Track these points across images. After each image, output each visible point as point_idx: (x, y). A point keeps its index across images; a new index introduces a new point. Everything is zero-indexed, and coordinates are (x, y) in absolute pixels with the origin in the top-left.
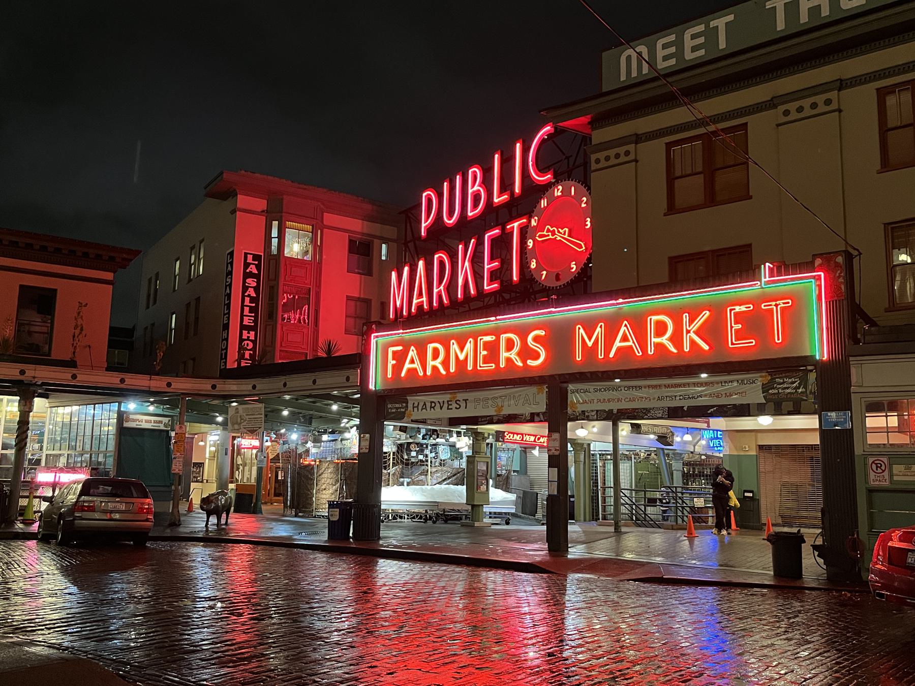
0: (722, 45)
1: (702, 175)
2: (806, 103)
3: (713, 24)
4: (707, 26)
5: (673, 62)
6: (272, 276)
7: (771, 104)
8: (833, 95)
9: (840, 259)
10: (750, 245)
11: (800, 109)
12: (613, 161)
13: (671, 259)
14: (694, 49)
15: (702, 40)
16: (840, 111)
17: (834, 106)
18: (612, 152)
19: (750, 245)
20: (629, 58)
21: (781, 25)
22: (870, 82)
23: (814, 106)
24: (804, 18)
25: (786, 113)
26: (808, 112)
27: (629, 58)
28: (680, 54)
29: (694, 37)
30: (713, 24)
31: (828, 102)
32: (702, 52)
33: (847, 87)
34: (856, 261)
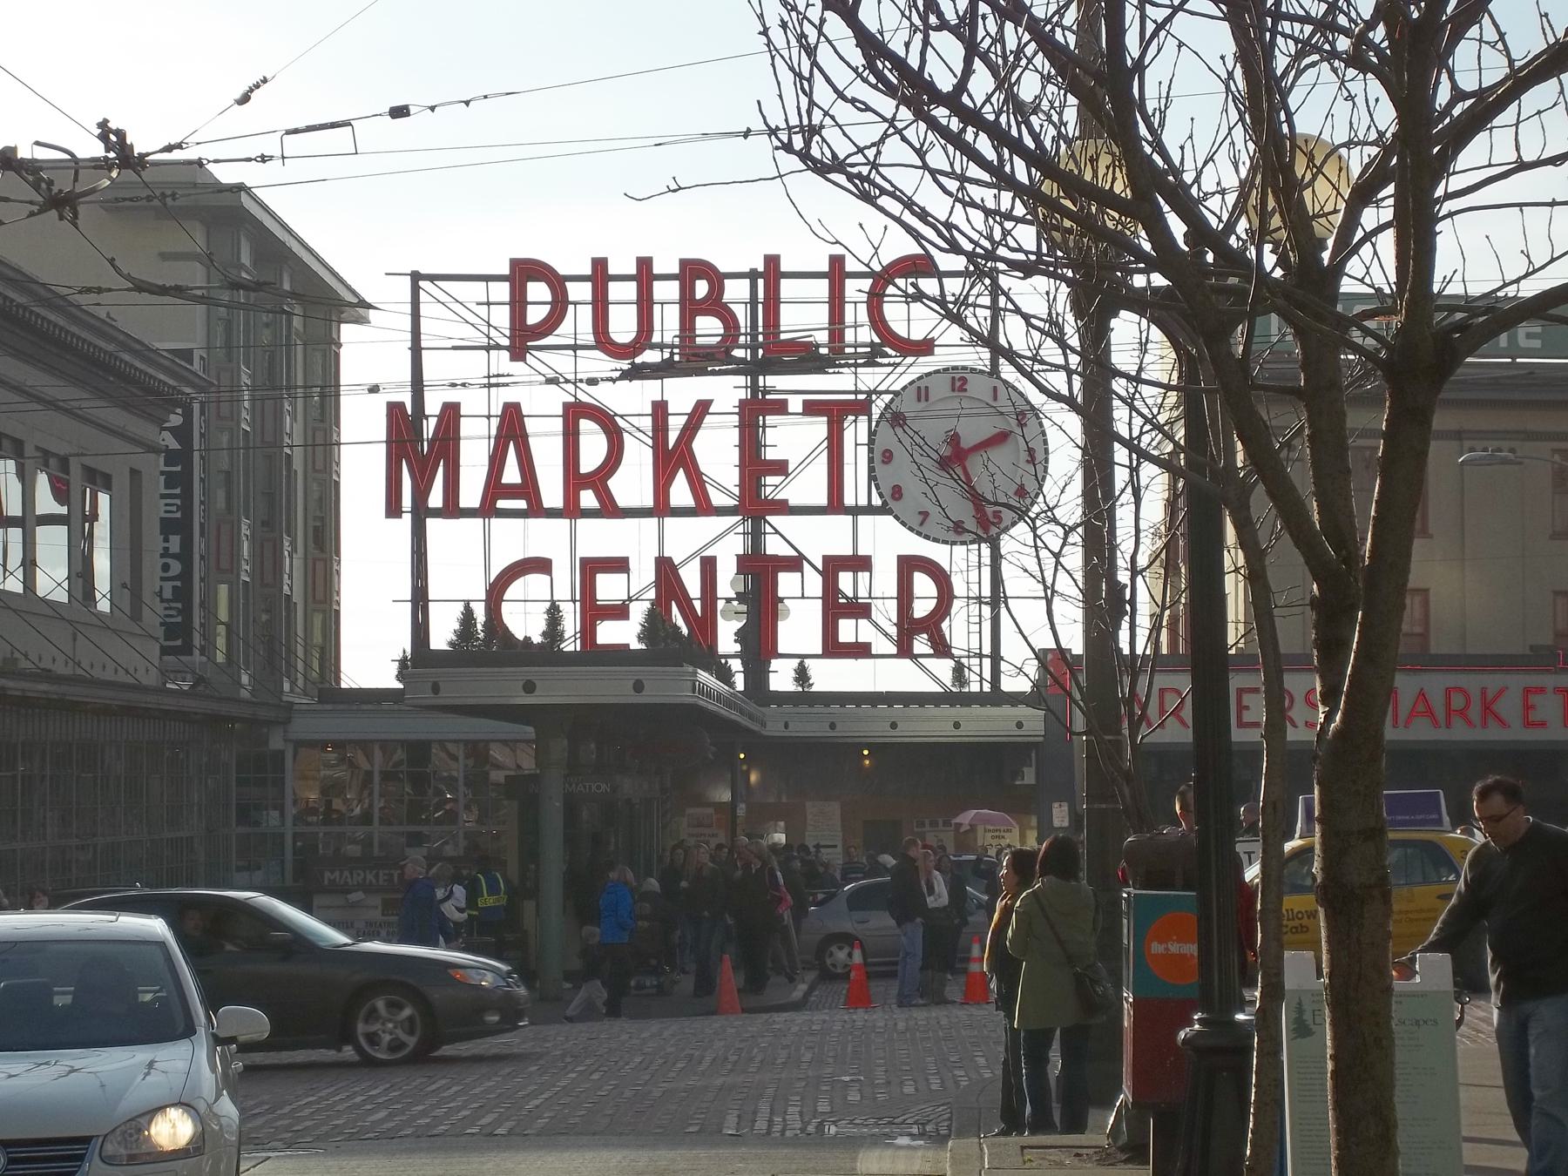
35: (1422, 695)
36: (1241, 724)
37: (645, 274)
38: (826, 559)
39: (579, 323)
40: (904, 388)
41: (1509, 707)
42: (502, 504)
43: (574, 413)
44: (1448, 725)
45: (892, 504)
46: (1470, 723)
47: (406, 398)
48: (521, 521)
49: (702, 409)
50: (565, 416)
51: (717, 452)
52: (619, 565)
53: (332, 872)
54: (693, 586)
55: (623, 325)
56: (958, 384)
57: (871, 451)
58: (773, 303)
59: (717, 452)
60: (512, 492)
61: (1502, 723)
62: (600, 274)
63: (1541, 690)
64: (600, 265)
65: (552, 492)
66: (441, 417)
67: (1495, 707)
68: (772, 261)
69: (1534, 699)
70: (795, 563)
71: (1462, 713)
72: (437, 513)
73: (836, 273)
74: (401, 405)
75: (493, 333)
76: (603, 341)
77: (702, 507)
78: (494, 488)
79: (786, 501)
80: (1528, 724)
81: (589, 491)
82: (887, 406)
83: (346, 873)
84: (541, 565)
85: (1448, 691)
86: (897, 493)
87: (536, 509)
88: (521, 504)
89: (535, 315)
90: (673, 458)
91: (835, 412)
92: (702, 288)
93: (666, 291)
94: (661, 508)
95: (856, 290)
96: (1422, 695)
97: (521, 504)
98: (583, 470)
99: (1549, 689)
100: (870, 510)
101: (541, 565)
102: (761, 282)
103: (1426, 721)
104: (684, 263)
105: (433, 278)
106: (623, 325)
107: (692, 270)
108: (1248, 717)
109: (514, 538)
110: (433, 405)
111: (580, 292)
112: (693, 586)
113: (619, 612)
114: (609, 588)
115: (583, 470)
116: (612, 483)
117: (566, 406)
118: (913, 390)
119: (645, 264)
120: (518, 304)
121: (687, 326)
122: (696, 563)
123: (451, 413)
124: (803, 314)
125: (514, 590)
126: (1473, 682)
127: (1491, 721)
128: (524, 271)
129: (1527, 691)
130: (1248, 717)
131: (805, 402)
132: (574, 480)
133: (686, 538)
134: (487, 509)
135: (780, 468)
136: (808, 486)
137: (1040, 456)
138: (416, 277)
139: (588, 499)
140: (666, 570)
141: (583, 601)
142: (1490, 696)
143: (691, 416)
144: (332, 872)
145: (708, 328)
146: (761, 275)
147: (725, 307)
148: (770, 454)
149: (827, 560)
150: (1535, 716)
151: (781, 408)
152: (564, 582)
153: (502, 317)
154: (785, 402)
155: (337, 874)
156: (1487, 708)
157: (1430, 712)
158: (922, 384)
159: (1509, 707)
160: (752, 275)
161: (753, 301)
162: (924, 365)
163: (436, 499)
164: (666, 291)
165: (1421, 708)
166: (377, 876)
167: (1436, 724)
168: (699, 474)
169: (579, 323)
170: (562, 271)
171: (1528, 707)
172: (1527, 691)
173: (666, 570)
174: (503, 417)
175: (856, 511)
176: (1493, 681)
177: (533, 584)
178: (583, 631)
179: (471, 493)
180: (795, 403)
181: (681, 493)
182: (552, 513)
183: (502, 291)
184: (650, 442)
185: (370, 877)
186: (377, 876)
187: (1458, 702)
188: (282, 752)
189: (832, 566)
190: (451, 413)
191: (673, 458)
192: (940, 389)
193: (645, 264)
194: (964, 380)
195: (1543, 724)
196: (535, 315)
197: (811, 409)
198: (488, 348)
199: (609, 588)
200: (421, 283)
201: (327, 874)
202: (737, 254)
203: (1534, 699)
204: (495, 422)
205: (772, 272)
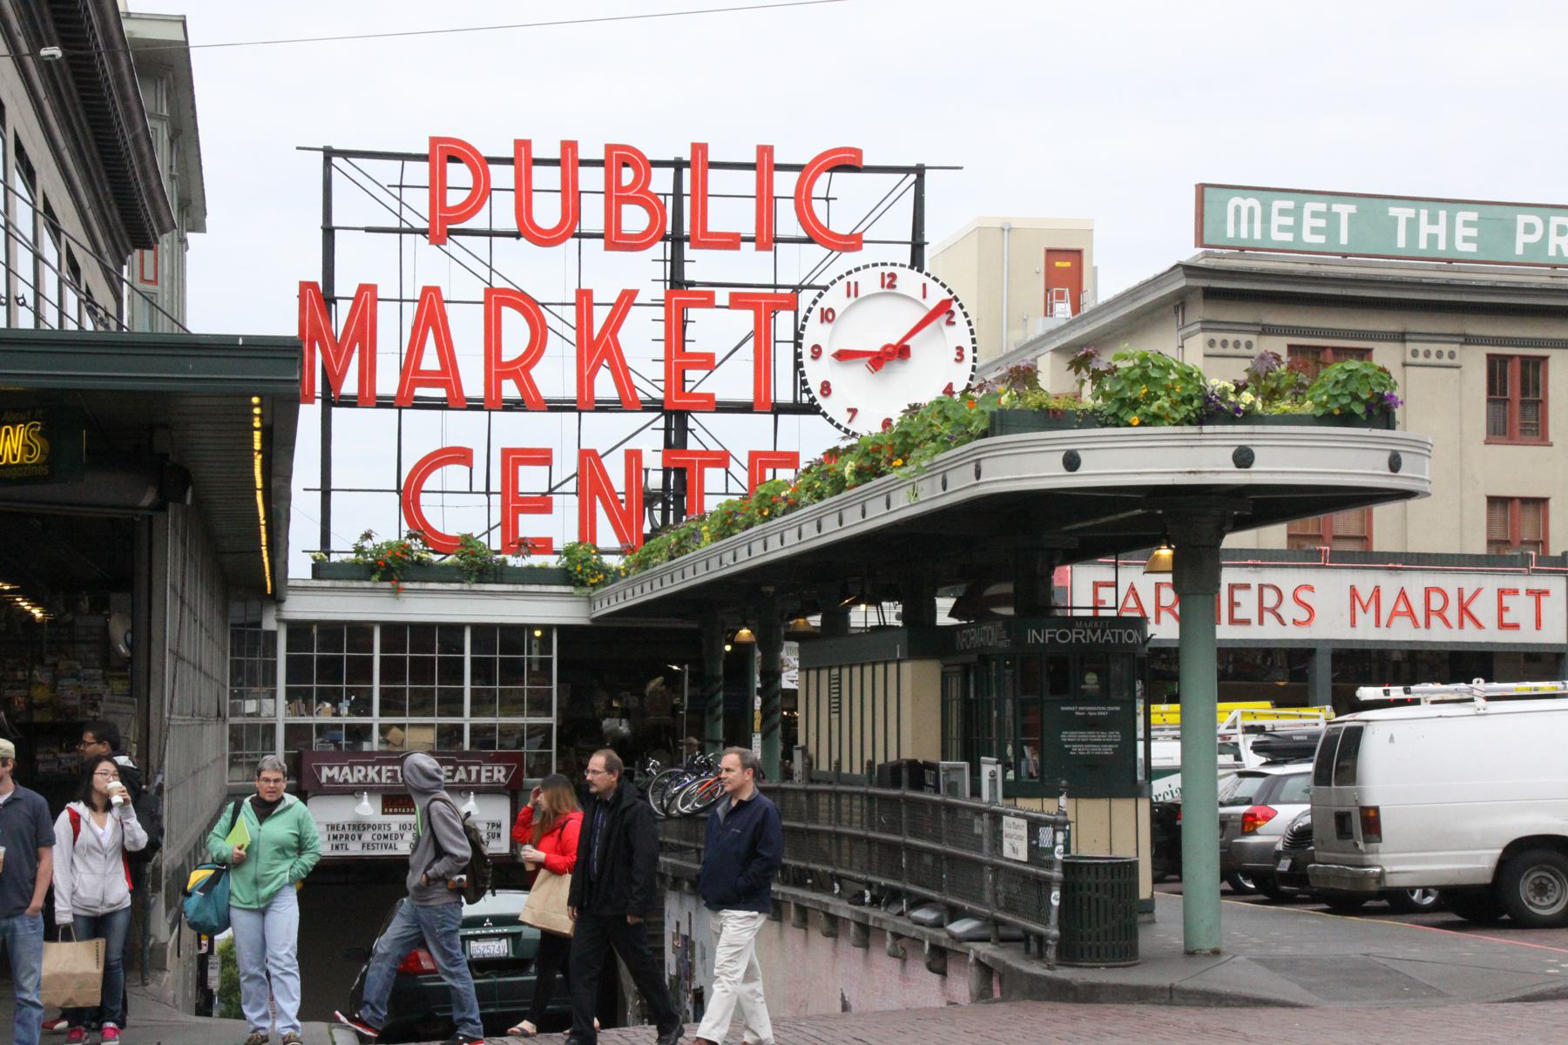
0: (1344, 239)
2: (1434, 348)
3: (1336, 208)
4: (1329, 208)
6: (149, 275)
7: (1401, 337)
11: (1427, 354)
12: (1230, 350)
14: (1315, 231)
15: (1321, 223)
18: (1231, 337)
20: (1238, 210)
21: (1401, 242)
23: (1439, 354)
24: (1423, 244)
25: (1415, 353)
26: (1433, 359)
27: (1238, 210)
28: (1297, 228)
29: (1315, 215)
32: (1321, 239)
35: (1403, 594)
36: (1233, 621)
37: (569, 159)
38: (753, 455)
39: (501, 211)
40: (833, 282)
41: (1484, 608)
42: (420, 392)
43: (497, 300)
44: (1428, 625)
45: (820, 400)
47: (317, 277)
48: (439, 412)
49: (627, 299)
50: (487, 303)
51: (642, 342)
52: (543, 457)
53: (331, 768)
54: (619, 484)
55: (547, 212)
56: (887, 280)
57: (797, 345)
58: (701, 195)
59: (642, 342)
60: (431, 380)
61: (1479, 626)
62: (523, 158)
63: (1516, 592)
64: (523, 145)
65: (473, 386)
66: (356, 300)
67: (1472, 608)
68: (699, 149)
69: (1507, 600)
70: (721, 459)
71: (1440, 613)
72: (349, 402)
73: (764, 164)
74: (314, 285)
75: (406, 214)
76: (526, 230)
77: (626, 403)
78: (411, 372)
79: (711, 396)
80: (1502, 625)
81: (513, 385)
82: (815, 302)
83: (346, 769)
84: (462, 456)
85: (1428, 591)
86: (826, 389)
87: (456, 402)
88: (441, 393)
89: (454, 199)
90: (597, 349)
91: (763, 303)
92: (628, 176)
93: (591, 179)
94: (585, 403)
95: (785, 183)
96: (1403, 594)
97: (441, 393)
98: (504, 359)
99: (1522, 592)
100: (796, 408)
101: (462, 456)
102: (687, 172)
103: (1407, 620)
104: (609, 148)
105: (346, 154)
106: (547, 212)
107: (619, 157)
108: (1239, 614)
109: (427, 431)
110: (345, 286)
111: (502, 176)
112: (619, 484)
113: (542, 504)
114: (531, 480)
115: (504, 359)
116: (533, 372)
117: (490, 291)
118: (842, 284)
119: (569, 146)
120: (438, 186)
121: (612, 217)
122: (620, 452)
123: (367, 296)
124: (730, 207)
125: (432, 482)
126: (1450, 582)
127: (1466, 620)
128: (447, 152)
129: (1501, 592)
130: (1239, 614)
131: (732, 295)
132: (496, 368)
133: (605, 432)
134: (403, 401)
135: (707, 362)
136: (733, 381)
137: (968, 354)
138: (329, 154)
139: (510, 390)
140: (589, 461)
141: (504, 493)
142: (1466, 599)
143: (616, 306)
144: (331, 768)
145: (635, 219)
146: (687, 164)
147: (655, 196)
148: (689, 348)
149: (753, 455)
150: (1508, 618)
151: (708, 302)
152: (487, 468)
153: (420, 201)
154: (711, 295)
155: (336, 770)
156: (1464, 609)
157: (1410, 613)
158: (852, 279)
159: (1484, 608)
160: (678, 165)
161: (678, 195)
162: (848, 260)
163: (350, 386)
164: (591, 179)
165: (1402, 608)
166: (379, 773)
167: (1416, 623)
168: (626, 369)
169: (501, 211)
170: (486, 152)
171: (1502, 609)
172: (1501, 592)
173: (589, 461)
174: (421, 302)
175: (778, 409)
176: (1469, 582)
177: (453, 475)
178: (504, 524)
179: (387, 382)
180: (722, 296)
181: (605, 386)
182: (474, 406)
183: (419, 172)
184: (572, 335)
185: (372, 772)
186: (379, 773)
187: (1436, 602)
188: (274, 634)
189: (759, 462)
190: (367, 296)
191: (597, 349)
192: (870, 282)
193: (569, 146)
194: (893, 276)
195: (1516, 626)
196: (454, 199)
197: (737, 302)
198: (400, 231)
199: (531, 480)
200: (336, 160)
201: (326, 772)
202: (663, 141)
203: (1507, 600)
204: (410, 310)
205: (697, 162)
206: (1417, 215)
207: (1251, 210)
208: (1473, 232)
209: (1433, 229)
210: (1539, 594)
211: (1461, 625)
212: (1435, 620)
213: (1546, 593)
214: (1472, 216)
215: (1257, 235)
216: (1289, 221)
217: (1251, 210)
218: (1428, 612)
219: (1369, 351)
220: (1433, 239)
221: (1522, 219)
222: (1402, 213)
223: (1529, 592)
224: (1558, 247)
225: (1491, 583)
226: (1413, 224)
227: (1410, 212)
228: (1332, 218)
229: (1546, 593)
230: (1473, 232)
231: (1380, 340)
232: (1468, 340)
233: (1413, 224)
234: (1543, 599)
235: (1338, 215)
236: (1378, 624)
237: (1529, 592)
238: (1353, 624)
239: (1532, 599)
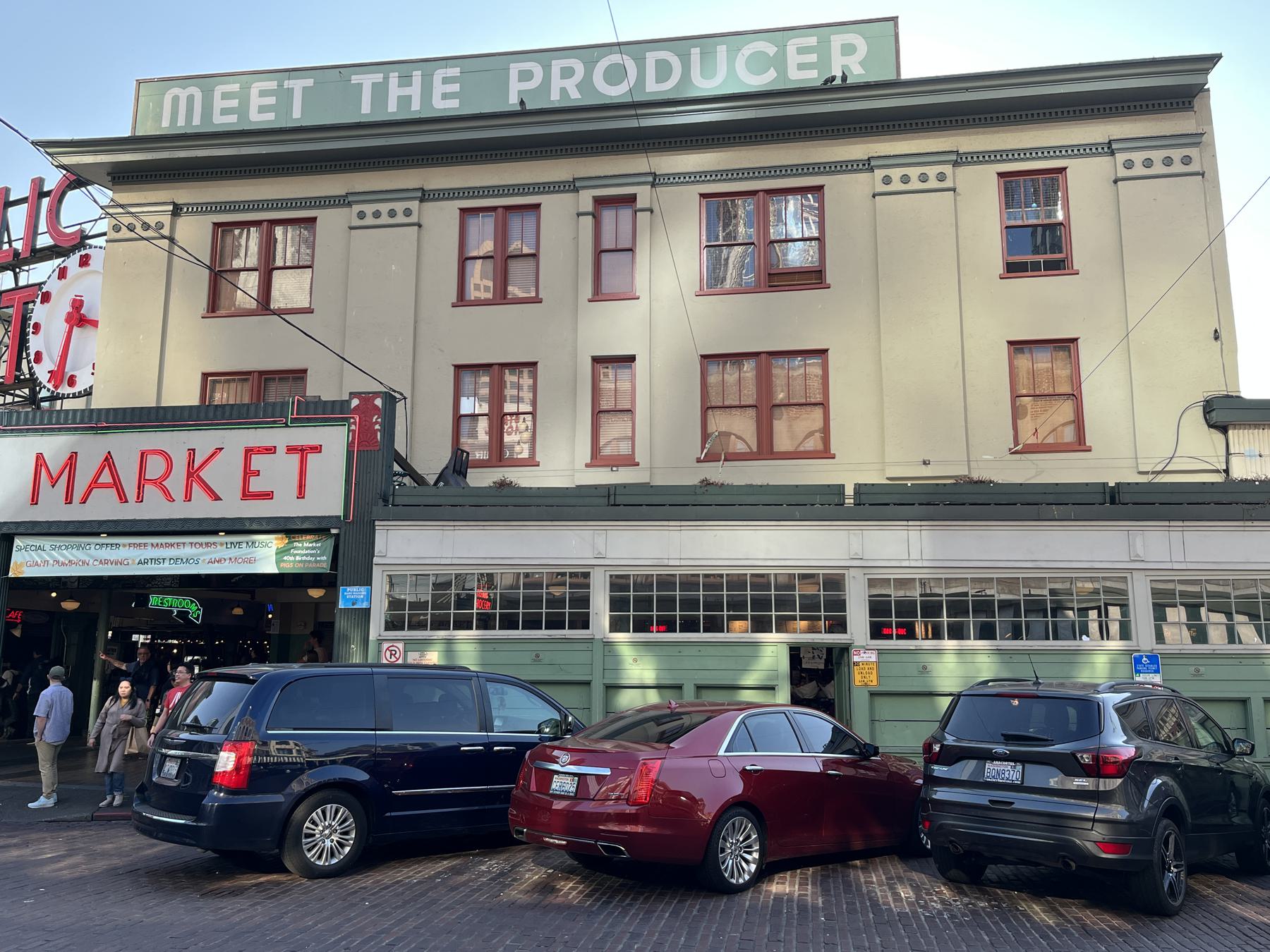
0: (297, 114)
1: (257, 273)
2: (384, 208)
3: (286, 84)
4: (280, 85)
5: (233, 119)
7: (343, 201)
8: (414, 205)
9: (378, 402)
10: (305, 371)
13: (205, 376)
14: (262, 109)
15: (271, 100)
16: (420, 226)
17: (413, 219)
19: (305, 371)
20: (176, 99)
22: (453, 199)
23: (392, 213)
24: (392, 107)
26: (385, 219)
27: (176, 99)
28: (243, 110)
30: (286, 84)
31: (408, 213)
32: (271, 116)
33: (429, 200)
34: (400, 406)
35: (108, 461)
44: (140, 499)
46: (166, 492)
63: (271, 450)
69: (257, 462)
71: (159, 483)
80: (247, 495)
96: (108, 461)
99: (281, 450)
126: (176, 442)
129: (249, 452)
150: (256, 485)
156: (193, 474)
157: (117, 484)
159: (224, 474)
165: (106, 477)
167: (123, 498)
171: (248, 473)
172: (249, 452)
176: (204, 440)
187: (155, 467)
195: (268, 495)
203: (257, 462)
206: (386, 78)
207: (190, 99)
208: (456, 87)
209: (406, 91)
210: (303, 452)
211: (188, 497)
212: (149, 489)
213: (317, 449)
214: (455, 72)
215: (196, 121)
216: (234, 103)
217: (190, 99)
218: (142, 482)
219: (314, 220)
220: (405, 101)
221: (515, 69)
222: (367, 81)
223: (291, 450)
224: (563, 91)
225: (236, 440)
226: (380, 91)
227: (378, 77)
228: (285, 96)
229: (317, 449)
230: (456, 87)
231: (325, 206)
232: (425, 196)
233: (380, 91)
234: (311, 457)
235: (290, 91)
236: (69, 500)
237: (291, 450)
238: (34, 500)
239: (296, 458)
